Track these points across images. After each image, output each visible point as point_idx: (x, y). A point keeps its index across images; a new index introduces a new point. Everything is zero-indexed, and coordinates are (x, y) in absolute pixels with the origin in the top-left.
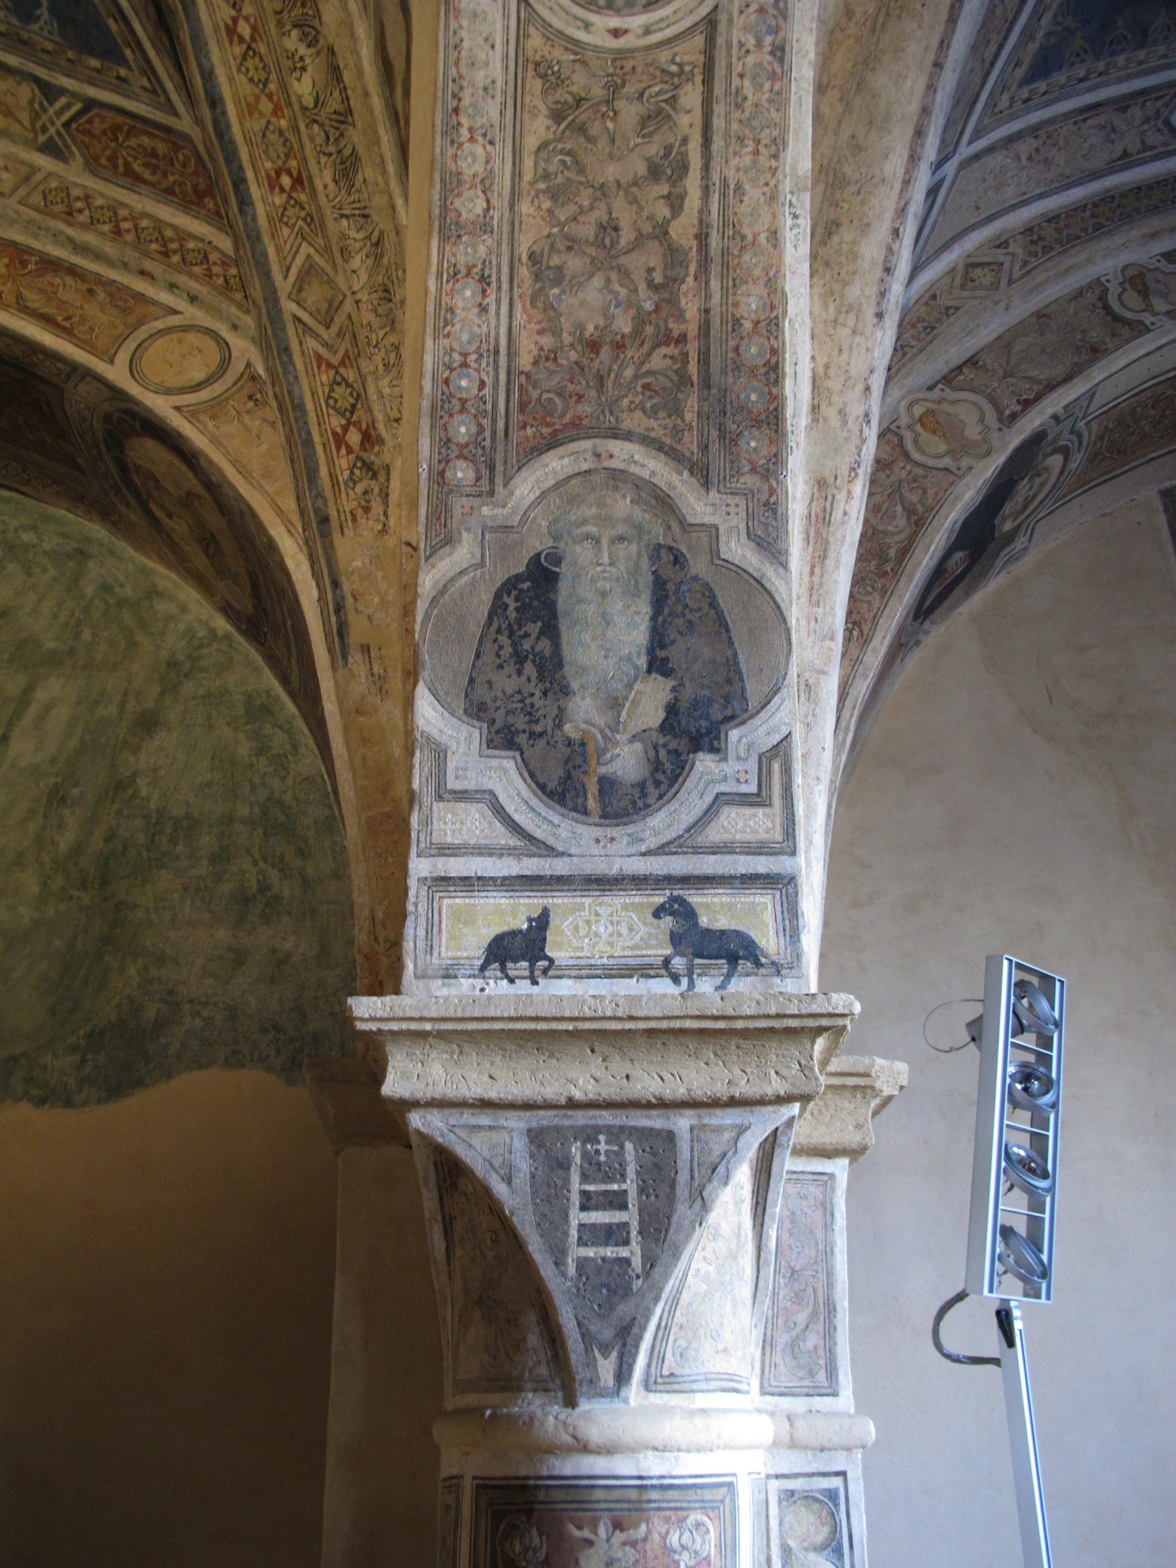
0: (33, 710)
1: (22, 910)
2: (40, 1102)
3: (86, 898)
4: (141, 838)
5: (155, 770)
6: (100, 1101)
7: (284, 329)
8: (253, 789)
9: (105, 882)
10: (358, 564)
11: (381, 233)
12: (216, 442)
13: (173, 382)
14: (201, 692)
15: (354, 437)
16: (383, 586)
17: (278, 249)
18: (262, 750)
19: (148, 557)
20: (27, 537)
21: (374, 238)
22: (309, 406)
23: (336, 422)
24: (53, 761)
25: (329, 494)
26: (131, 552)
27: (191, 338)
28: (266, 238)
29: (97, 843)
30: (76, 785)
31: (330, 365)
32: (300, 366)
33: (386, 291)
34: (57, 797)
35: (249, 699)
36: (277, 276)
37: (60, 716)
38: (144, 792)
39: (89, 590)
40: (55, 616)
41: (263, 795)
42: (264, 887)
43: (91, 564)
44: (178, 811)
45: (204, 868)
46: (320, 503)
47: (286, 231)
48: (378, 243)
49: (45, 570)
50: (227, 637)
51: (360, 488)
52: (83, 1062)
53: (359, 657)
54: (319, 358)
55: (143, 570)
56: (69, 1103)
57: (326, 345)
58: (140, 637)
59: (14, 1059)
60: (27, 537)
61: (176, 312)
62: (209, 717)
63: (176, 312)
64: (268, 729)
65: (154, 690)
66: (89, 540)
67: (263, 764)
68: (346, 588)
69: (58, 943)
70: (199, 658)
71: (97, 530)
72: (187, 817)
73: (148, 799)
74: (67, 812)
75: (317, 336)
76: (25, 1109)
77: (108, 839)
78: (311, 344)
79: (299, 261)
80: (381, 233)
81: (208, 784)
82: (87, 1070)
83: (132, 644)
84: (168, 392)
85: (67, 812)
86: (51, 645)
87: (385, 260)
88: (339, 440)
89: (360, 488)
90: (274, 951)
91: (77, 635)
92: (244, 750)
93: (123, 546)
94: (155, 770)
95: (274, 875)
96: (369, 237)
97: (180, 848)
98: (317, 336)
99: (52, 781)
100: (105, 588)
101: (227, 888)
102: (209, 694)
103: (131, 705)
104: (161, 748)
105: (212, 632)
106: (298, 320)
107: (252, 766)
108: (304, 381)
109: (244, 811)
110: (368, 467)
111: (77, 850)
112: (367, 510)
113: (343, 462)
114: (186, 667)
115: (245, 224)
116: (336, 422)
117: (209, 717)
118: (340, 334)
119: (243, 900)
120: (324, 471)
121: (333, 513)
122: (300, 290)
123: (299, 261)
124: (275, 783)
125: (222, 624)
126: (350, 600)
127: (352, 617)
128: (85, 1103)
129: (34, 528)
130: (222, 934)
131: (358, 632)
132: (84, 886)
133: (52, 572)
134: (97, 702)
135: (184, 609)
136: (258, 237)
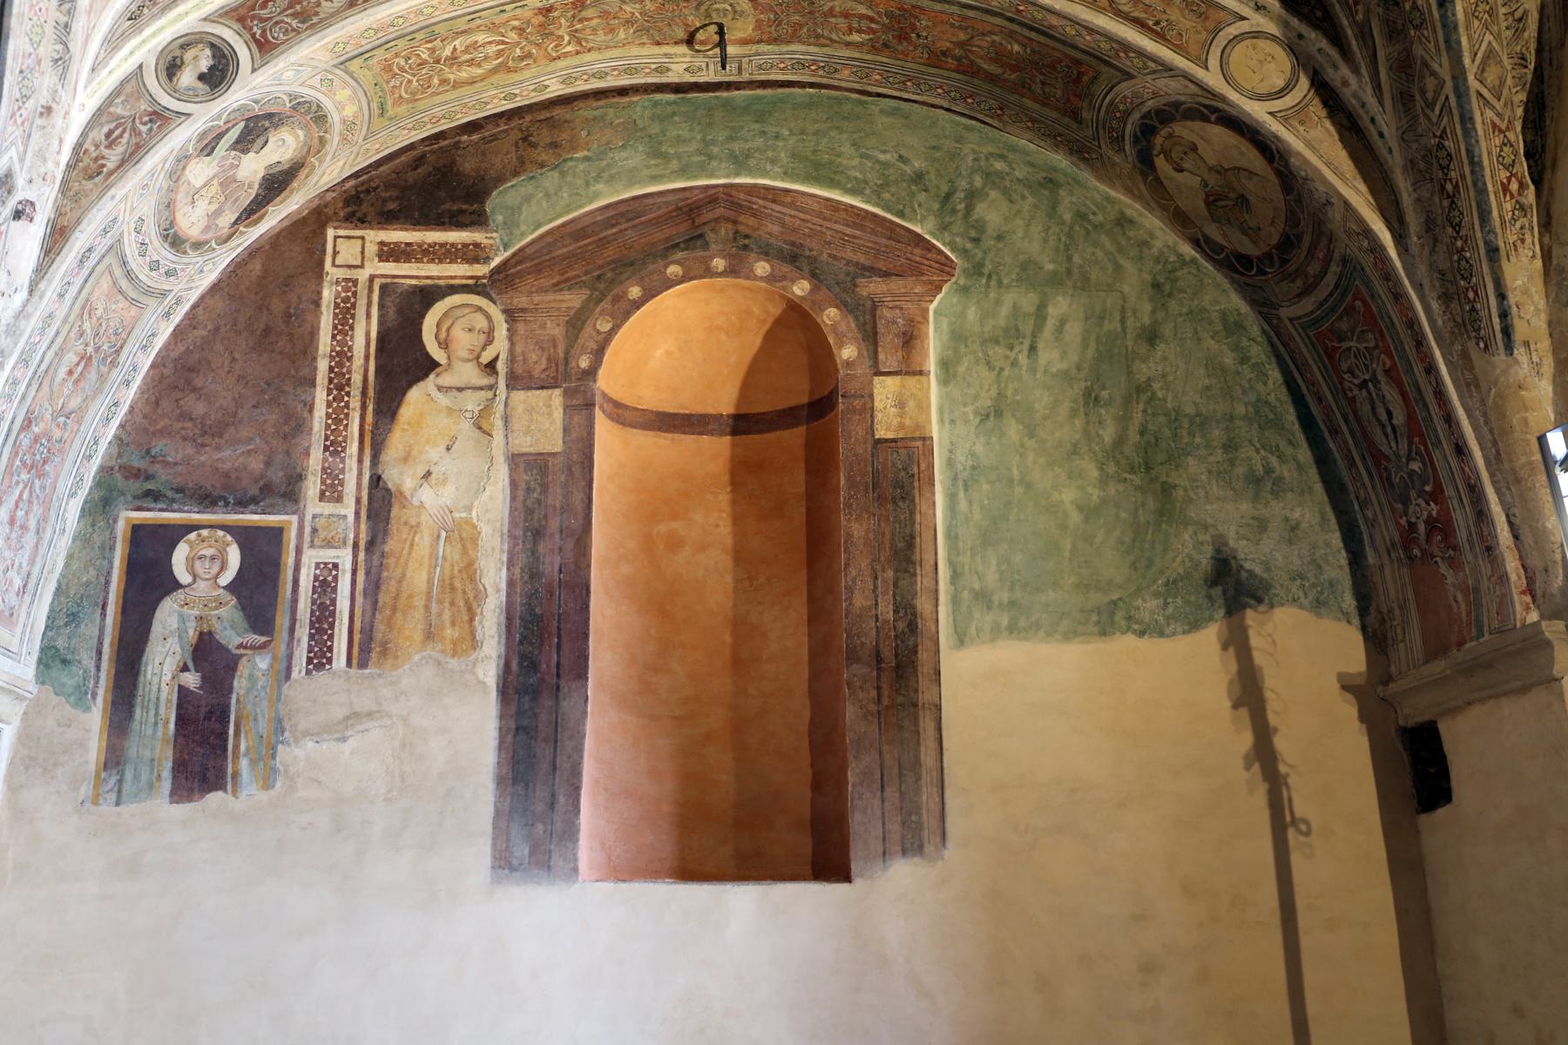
0: (1050, 324)
1: (1090, 490)
2: (1142, 634)
3: (1137, 480)
4: (1167, 433)
5: (1164, 376)
6: (1184, 632)
7: (1469, 102)
8: (1244, 392)
9: (1148, 468)
10: (1519, 282)
11: (1526, 12)
12: (1308, 144)
13: (1262, 89)
14: (1185, 310)
15: (1514, 186)
16: (1536, 298)
17: (1470, 38)
18: (1244, 360)
19: (1112, 186)
20: (999, 165)
21: (1518, 15)
22: (1486, 163)
23: (1504, 174)
24: (1079, 368)
25: (1498, 230)
26: (1093, 182)
27: (1261, 43)
28: (1461, 30)
29: (1133, 437)
30: (1104, 388)
31: (1501, 131)
32: (1480, 132)
33: (1523, 58)
34: (1091, 399)
35: (1224, 315)
36: (1467, 61)
37: (1074, 330)
38: (1160, 394)
39: (1068, 217)
40: (1045, 240)
41: (1253, 397)
42: (1269, 471)
43: (1062, 193)
44: (1189, 410)
45: (1219, 456)
46: (1492, 237)
47: (1476, 23)
48: (1520, 20)
49: (1023, 197)
50: (1193, 261)
51: (1518, 225)
52: (1166, 604)
53: (1522, 350)
54: (1494, 125)
55: (1108, 198)
56: (1162, 634)
57: (1498, 114)
58: (1123, 262)
59: (1114, 603)
60: (999, 165)
61: (1243, 18)
62: (1196, 332)
63: (1243, 18)
64: (1245, 343)
65: (1148, 307)
66: (1054, 169)
67: (1246, 369)
68: (1512, 299)
69: (1124, 515)
70: (1176, 280)
71: (1060, 160)
72: (1199, 414)
73: (1165, 401)
74: (1103, 412)
75: (1493, 108)
76: (1130, 640)
77: (1142, 433)
78: (1489, 114)
79: (1483, 48)
80: (1526, 12)
81: (1208, 388)
82: (1170, 610)
83: (1118, 268)
84: (1260, 98)
85: (1103, 412)
86: (1050, 267)
87: (1526, 34)
88: (1506, 188)
89: (1518, 225)
90: (1287, 519)
91: (1069, 259)
92: (1229, 359)
93: (1085, 175)
94: (1164, 376)
95: (1274, 461)
96: (1512, 14)
97: (1198, 440)
98: (1493, 108)
99: (1083, 384)
100: (1081, 216)
101: (1240, 470)
102: (1191, 312)
103: (1130, 323)
104: (1165, 359)
105: (1180, 255)
106: (1480, 94)
107: (1238, 373)
108: (1483, 144)
109: (1240, 409)
110: (1522, 208)
111: (1119, 442)
112: (1523, 241)
113: (1508, 206)
114: (1167, 288)
115: (1443, 17)
116: (1504, 174)
117: (1196, 332)
118: (1506, 105)
119: (1255, 481)
120: (1495, 213)
121: (1501, 244)
122: (1483, 71)
123: (1483, 48)
124: (1260, 386)
125: (1187, 250)
126: (1514, 309)
127: (1516, 321)
128: (1174, 634)
129: (1002, 157)
130: (1245, 507)
131: (1520, 331)
132: (1132, 470)
133: (1030, 200)
134: (1102, 318)
135: (1152, 236)
136: (1456, 28)
